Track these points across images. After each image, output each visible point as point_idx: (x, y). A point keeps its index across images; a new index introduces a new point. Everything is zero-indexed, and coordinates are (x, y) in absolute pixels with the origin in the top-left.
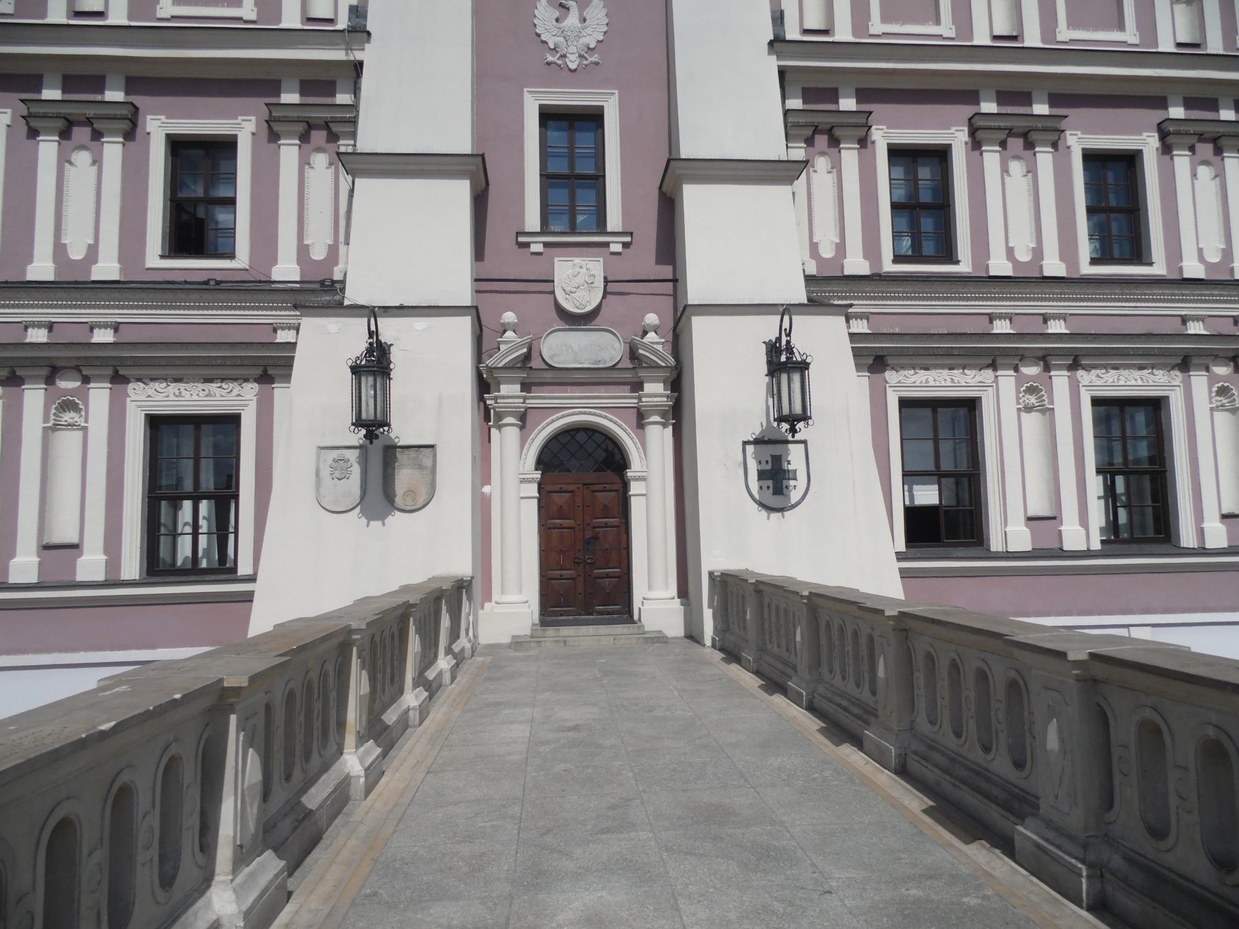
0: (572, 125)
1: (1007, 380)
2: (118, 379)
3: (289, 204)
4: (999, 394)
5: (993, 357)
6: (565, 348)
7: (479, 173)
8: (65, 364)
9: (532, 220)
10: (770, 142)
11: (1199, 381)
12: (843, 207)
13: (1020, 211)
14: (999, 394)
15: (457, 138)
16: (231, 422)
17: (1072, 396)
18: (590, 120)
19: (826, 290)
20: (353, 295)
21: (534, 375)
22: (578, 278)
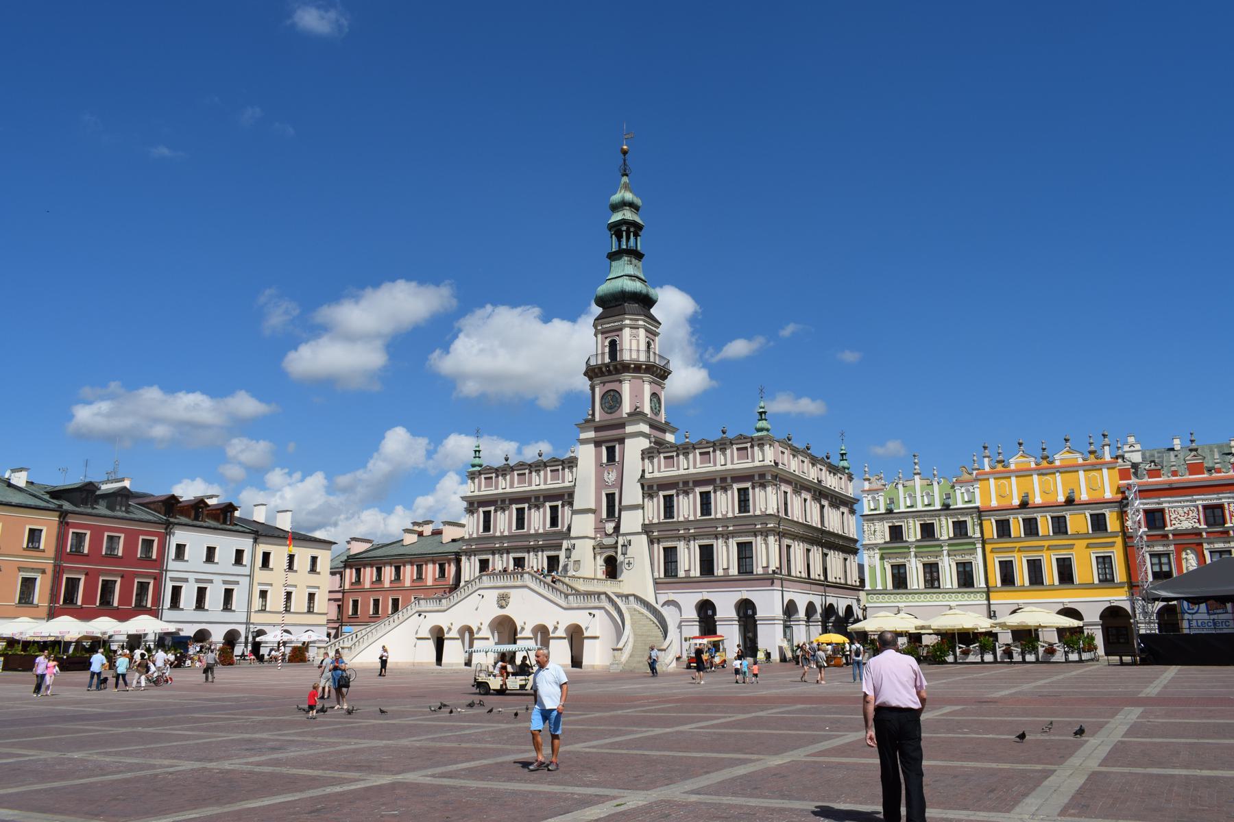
4: (681, 546)
5: (679, 538)
11: (720, 541)
12: (654, 510)
13: (687, 507)
14: (681, 546)
19: (647, 529)
20: (573, 534)
21: (602, 547)
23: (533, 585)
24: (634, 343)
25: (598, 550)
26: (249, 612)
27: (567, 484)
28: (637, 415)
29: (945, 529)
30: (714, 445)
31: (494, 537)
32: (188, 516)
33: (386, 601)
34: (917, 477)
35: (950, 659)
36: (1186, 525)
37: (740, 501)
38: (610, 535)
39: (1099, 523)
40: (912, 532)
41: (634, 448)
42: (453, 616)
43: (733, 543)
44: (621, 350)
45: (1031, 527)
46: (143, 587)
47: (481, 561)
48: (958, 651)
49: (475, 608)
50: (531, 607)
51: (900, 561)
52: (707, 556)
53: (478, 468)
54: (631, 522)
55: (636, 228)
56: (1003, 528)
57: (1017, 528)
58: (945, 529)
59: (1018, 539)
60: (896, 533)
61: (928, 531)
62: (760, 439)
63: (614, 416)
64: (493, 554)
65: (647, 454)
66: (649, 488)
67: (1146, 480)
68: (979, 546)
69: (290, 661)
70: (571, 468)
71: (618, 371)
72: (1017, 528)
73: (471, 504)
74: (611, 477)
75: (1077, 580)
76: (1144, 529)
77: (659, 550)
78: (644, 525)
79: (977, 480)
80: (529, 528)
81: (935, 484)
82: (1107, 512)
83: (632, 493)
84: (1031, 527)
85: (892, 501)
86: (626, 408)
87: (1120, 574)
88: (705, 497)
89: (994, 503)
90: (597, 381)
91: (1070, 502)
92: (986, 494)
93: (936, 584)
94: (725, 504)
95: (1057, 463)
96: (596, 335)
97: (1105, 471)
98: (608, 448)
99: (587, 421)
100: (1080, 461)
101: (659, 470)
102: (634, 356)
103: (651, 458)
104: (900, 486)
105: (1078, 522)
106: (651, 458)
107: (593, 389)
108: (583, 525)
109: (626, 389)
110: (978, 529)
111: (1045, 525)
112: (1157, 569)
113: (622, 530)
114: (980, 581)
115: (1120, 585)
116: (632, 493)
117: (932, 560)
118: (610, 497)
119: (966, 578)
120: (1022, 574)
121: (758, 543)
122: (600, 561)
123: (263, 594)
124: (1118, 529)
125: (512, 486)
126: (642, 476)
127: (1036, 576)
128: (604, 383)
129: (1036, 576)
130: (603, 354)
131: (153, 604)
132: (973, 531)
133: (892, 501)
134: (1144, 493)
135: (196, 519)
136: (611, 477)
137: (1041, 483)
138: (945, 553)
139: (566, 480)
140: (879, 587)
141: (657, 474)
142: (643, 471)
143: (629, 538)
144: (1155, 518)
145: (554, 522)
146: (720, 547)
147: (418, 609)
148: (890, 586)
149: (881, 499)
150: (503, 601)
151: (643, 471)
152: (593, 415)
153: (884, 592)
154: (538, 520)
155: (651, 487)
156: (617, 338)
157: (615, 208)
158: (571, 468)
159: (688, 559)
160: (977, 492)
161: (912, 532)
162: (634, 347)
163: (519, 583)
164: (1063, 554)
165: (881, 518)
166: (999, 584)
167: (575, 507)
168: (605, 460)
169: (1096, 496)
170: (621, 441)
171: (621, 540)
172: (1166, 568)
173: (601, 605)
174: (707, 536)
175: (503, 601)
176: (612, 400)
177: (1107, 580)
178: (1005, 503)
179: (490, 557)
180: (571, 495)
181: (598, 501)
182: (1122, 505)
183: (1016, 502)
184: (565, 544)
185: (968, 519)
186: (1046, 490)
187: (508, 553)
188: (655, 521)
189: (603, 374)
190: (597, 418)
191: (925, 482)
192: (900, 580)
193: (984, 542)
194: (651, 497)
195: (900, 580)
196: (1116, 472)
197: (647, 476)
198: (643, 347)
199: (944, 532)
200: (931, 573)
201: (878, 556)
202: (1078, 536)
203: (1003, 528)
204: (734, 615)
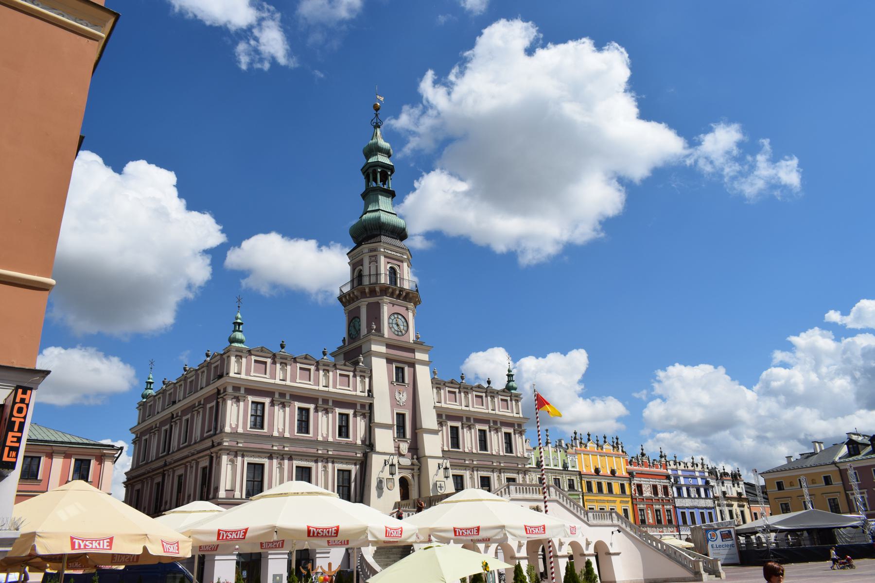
1: (468, 472)
2: (333, 462)
3: (358, 427)
5: (466, 467)
8: (326, 459)
10: (435, 426)
13: (469, 440)
16: (262, 465)
18: (403, 415)
31: (270, 437)
38: (403, 456)
41: (423, 374)
61: (557, 482)
63: (401, 338)
65: (437, 384)
66: (443, 416)
74: (404, 397)
79: (576, 453)
90: (386, 299)
108: (384, 440)
118: (401, 417)
128: (393, 305)
132: (577, 486)
139: (356, 389)
144: (639, 487)
145: (344, 430)
152: (379, 330)
154: (324, 426)
170: (412, 365)
179: (265, 461)
190: (386, 335)
202: (617, 496)
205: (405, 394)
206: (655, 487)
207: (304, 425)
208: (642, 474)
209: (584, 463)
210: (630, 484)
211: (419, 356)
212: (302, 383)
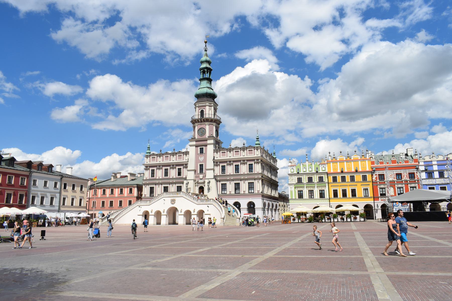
0: (201, 166)
3: (185, 173)
5: (227, 180)
6: (200, 181)
7: (195, 171)
8: (172, 183)
9: (199, 172)
11: (242, 181)
12: (218, 170)
13: (230, 170)
14: (228, 183)
15: (193, 168)
17: (233, 183)
19: (215, 177)
21: (198, 183)
22: (201, 176)
23: (184, 196)
24: (210, 111)
25: (197, 184)
26: (59, 206)
27: (184, 161)
28: (211, 137)
29: (315, 179)
30: (240, 149)
31: (156, 179)
32: (35, 169)
33: (107, 202)
34: (307, 162)
35: (323, 221)
36: (391, 179)
37: (249, 168)
39: (364, 178)
40: (305, 180)
41: (210, 149)
42: (152, 207)
43: (247, 182)
44: (206, 114)
45: (343, 179)
46: (21, 196)
47: (150, 187)
48: (326, 218)
49: (162, 204)
50: (184, 204)
51: (301, 189)
52: (237, 186)
53: (149, 154)
54: (210, 174)
55: (209, 70)
56: (335, 179)
57: (339, 179)
58: (315, 179)
59: (339, 182)
60: (300, 180)
61: (310, 180)
62: (257, 147)
64: (156, 185)
66: (216, 163)
67: (379, 165)
68: (327, 185)
69: (81, 224)
70: (186, 155)
71: (204, 121)
72: (339, 179)
73: (147, 167)
75: (357, 196)
76: (378, 180)
77: (219, 184)
78: (214, 176)
79: (327, 163)
80: (170, 176)
81: (313, 164)
82: (367, 175)
83: (210, 164)
84: (343, 179)
85: (298, 169)
86: (207, 135)
87: (370, 194)
88: (237, 167)
89: (332, 171)
90: (196, 124)
91: (356, 171)
92: (329, 168)
93: (313, 197)
94: (244, 169)
95: (352, 159)
96: (195, 108)
97: (367, 162)
98: (200, 148)
99: (192, 138)
100: (359, 158)
101: (219, 156)
102: (210, 116)
103: (217, 152)
104: (301, 165)
105: (358, 177)
106: (217, 152)
107: (194, 127)
108: (190, 175)
109: (207, 128)
110: (327, 179)
111: (348, 179)
112: (381, 193)
113: (207, 177)
114: (327, 196)
115: (371, 197)
116: (210, 164)
117: (312, 189)
118: (201, 166)
119: (322, 195)
120: (340, 194)
121: (256, 182)
122: (197, 188)
123: (64, 199)
124: (371, 180)
125: (163, 161)
126: (214, 159)
127: (344, 195)
129: (344, 195)
130: (198, 115)
131: (25, 202)
132: (325, 179)
133: (298, 169)
134: (378, 169)
135: (38, 170)
136: (201, 158)
137: (347, 165)
138: (316, 187)
139: (184, 159)
140: (294, 198)
141: (219, 158)
142: (214, 157)
143: (210, 180)
144: (382, 177)
145: (179, 174)
146: (241, 183)
147: (138, 204)
148: (297, 197)
149: (295, 169)
150: (173, 201)
151: (214, 157)
153: (295, 199)
154: (173, 173)
155: (217, 163)
156: (204, 110)
157: (202, 62)
158: (186, 155)
159: (230, 187)
160: (327, 167)
161: (305, 180)
162: (210, 113)
163: (179, 195)
164: (353, 188)
165: (295, 175)
166: (333, 197)
167: (188, 169)
168: (199, 153)
169: (364, 170)
171: (207, 181)
172: (384, 193)
173: (211, 203)
174: (238, 180)
175: (173, 201)
176: (202, 132)
177: (366, 196)
178: (335, 171)
179: (154, 186)
180: (186, 165)
181: (196, 166)
182: (372, 172)
183: (339, 171)
184: (185, 182)
185: (323, 176)
186: (349, 167)
187: (162, 184)
188: (218, 174)
189: (199, 122)
191: (310, 164)
192: (301, 196)
193: (328, 183)
194: (217, 165)
195: (301, 196)
196: (370, 162)
197: (215, 159)
198: (213, 113)
199: (316, 180)
200: (311, 193)
201: (293, 188)
203: (335, 179)
204: (246, 207)
205: (203, 158)
206: (399, 175)
207: (166, 174)
208: (378, 169)
209: (332, 168)
210: (372, 175)
211: (209, 142)
212: (166, 162)
